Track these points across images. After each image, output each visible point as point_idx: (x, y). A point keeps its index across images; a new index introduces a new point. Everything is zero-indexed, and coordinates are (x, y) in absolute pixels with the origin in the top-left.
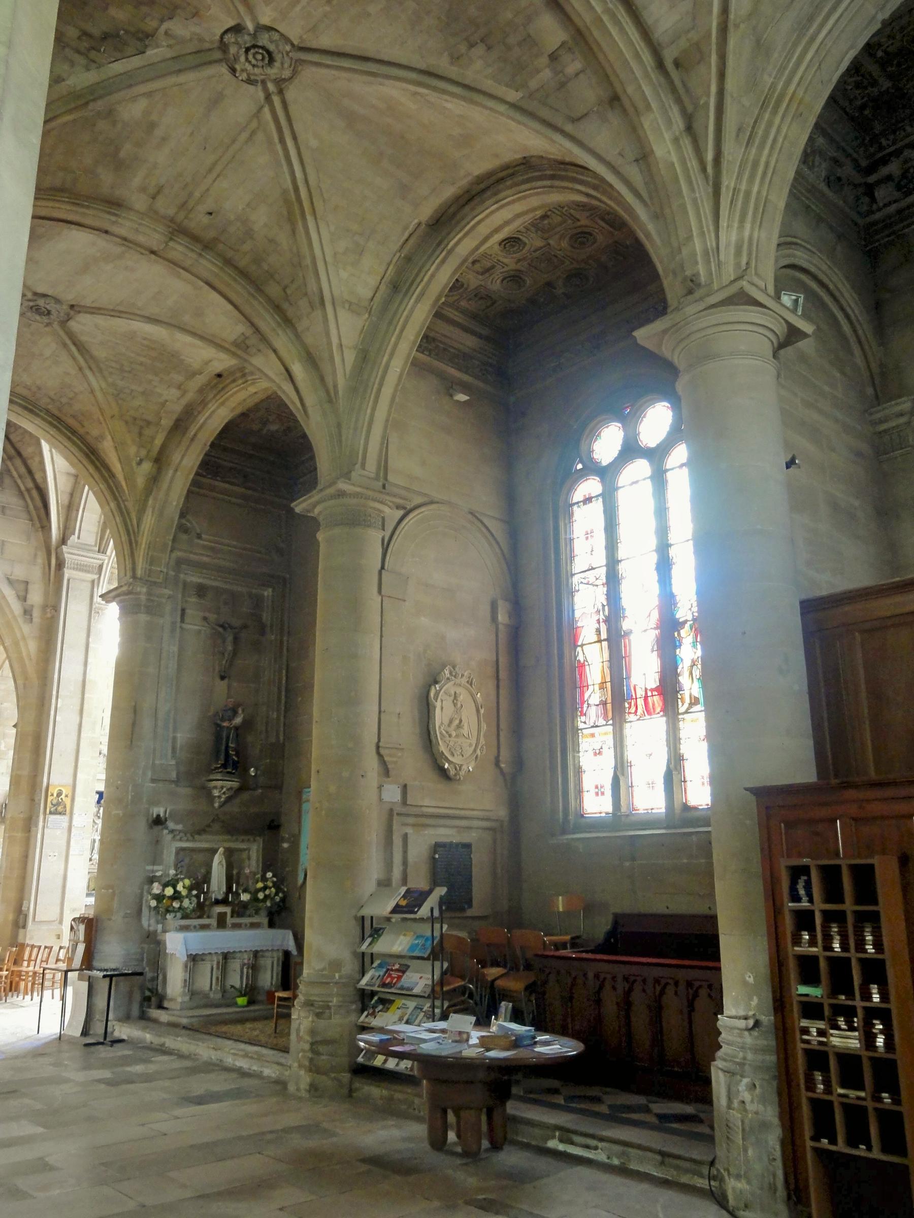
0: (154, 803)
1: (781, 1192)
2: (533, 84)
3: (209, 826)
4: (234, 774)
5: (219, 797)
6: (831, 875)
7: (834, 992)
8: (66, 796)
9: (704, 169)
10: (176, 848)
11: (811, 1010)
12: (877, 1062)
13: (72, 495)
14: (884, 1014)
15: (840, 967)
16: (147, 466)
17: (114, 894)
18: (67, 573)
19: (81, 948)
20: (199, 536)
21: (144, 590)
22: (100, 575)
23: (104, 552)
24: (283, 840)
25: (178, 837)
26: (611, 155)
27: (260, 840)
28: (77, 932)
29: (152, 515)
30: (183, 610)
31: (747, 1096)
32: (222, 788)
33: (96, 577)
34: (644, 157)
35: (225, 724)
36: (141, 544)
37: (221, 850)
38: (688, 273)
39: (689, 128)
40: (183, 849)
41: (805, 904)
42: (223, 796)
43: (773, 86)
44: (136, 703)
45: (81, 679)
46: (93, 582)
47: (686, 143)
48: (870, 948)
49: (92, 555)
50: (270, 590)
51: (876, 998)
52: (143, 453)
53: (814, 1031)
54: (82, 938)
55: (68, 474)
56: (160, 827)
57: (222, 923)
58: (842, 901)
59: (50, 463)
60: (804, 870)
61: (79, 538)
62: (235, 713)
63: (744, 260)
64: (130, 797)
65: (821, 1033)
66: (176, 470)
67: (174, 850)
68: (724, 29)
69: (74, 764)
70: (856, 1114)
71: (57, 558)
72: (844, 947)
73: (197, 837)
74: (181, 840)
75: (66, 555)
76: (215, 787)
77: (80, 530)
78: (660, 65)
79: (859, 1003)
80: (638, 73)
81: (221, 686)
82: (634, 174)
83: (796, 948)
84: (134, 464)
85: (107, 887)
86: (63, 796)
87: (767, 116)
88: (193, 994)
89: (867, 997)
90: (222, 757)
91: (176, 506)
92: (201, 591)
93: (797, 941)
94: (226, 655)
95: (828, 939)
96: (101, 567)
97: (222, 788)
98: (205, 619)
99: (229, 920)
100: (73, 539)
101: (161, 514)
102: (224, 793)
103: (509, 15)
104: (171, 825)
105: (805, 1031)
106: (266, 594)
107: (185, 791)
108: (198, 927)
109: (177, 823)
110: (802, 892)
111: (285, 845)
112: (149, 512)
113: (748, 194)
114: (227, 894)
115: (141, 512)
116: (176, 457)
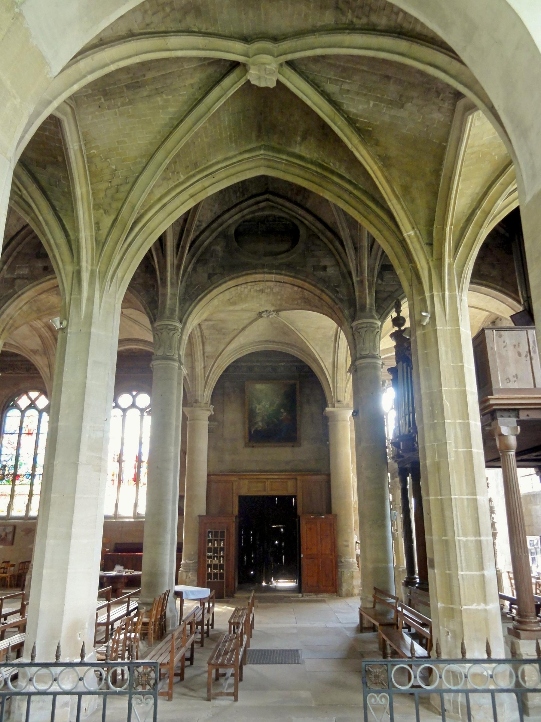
6: (216, 533)
7: (214, 553)
11: (210, 557)
12: (220, 565)
14: (223, 557)
15: (216, 549)
31: (190, 576)
38: (197, 398)
39: (204, 368)
41: (210, 538)
47: (203, 370)
48: (222, 546)
58: (218, 537)
60: (212, 532)
68: (219, 356)
70: (216, 574)
78: (204, 354)
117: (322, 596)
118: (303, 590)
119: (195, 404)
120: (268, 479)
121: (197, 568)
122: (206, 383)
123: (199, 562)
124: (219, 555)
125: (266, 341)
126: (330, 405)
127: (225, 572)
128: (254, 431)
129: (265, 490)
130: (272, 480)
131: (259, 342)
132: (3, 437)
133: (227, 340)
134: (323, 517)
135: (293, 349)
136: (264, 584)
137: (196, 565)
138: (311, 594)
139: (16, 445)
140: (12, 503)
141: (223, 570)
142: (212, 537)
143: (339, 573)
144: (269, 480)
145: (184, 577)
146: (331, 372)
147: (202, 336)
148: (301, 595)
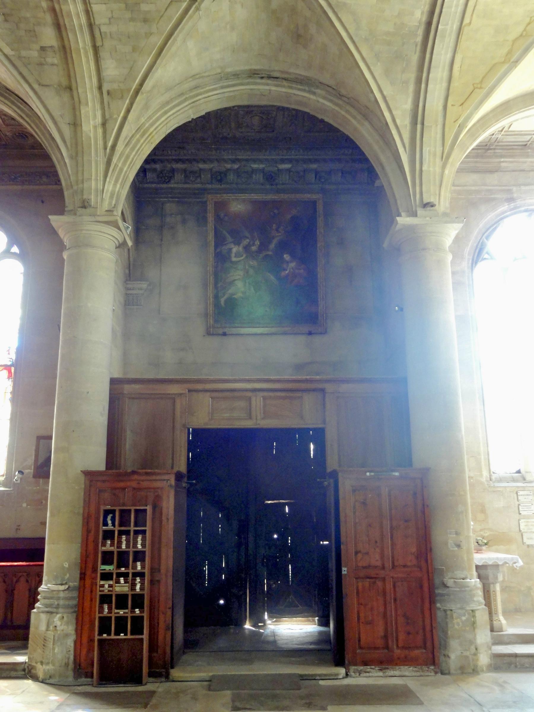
1: (71, 666)
2: (24, 53)
6: (125, 513)
7: (119, 567)
9: (105, 148)
14: (141, 575)
26: (56, 114)
34: (76, 125)
38: (85, 197)
41: (110, 527)
43: (144, 124)
47: (100, 131)
48: (139, 546)
51: (139, 568)
53: (106, 586)
58: (130, 526)
60: (113, 512)
63: (114, 202)
65: (110, 586)
68: (137, 92)
72: (128, 546)
78: (100, 88)
79: (131, 571)
80: (88, 85)
82: (67, 131)
83: (103, 548)
87: (138, 136)
89: (135, 567)
93: (104, 545)
95: (120, 543)
103: (28, 15)
105: (103, 586)
110: (110, 522)
113: (121, 170)
117: (397, 673)
118: (348, 657)
119: (81, 211)
120: (255, 390)
121: (75, 602)
122: (109, 163)
123: (81, 589)
124: (131, 571)
125: (253, 74)
126: (403, 214)
127: (146, 615)
128: (226, 301)
129: (250, 418)
130: (266, 394)
131: (236, 75)
133: (157, 40)
134: (397, 474)
135: (314, 93)
136: (248, 626)
137: (75, 594)
138: (368, 668)
141: (142, 611)
142: (114, 525)
143: (440, 614)
144: (262, 394)
145: (43, 627)
146: (406, 136)
147: (91, 26)
148: (342, 671)
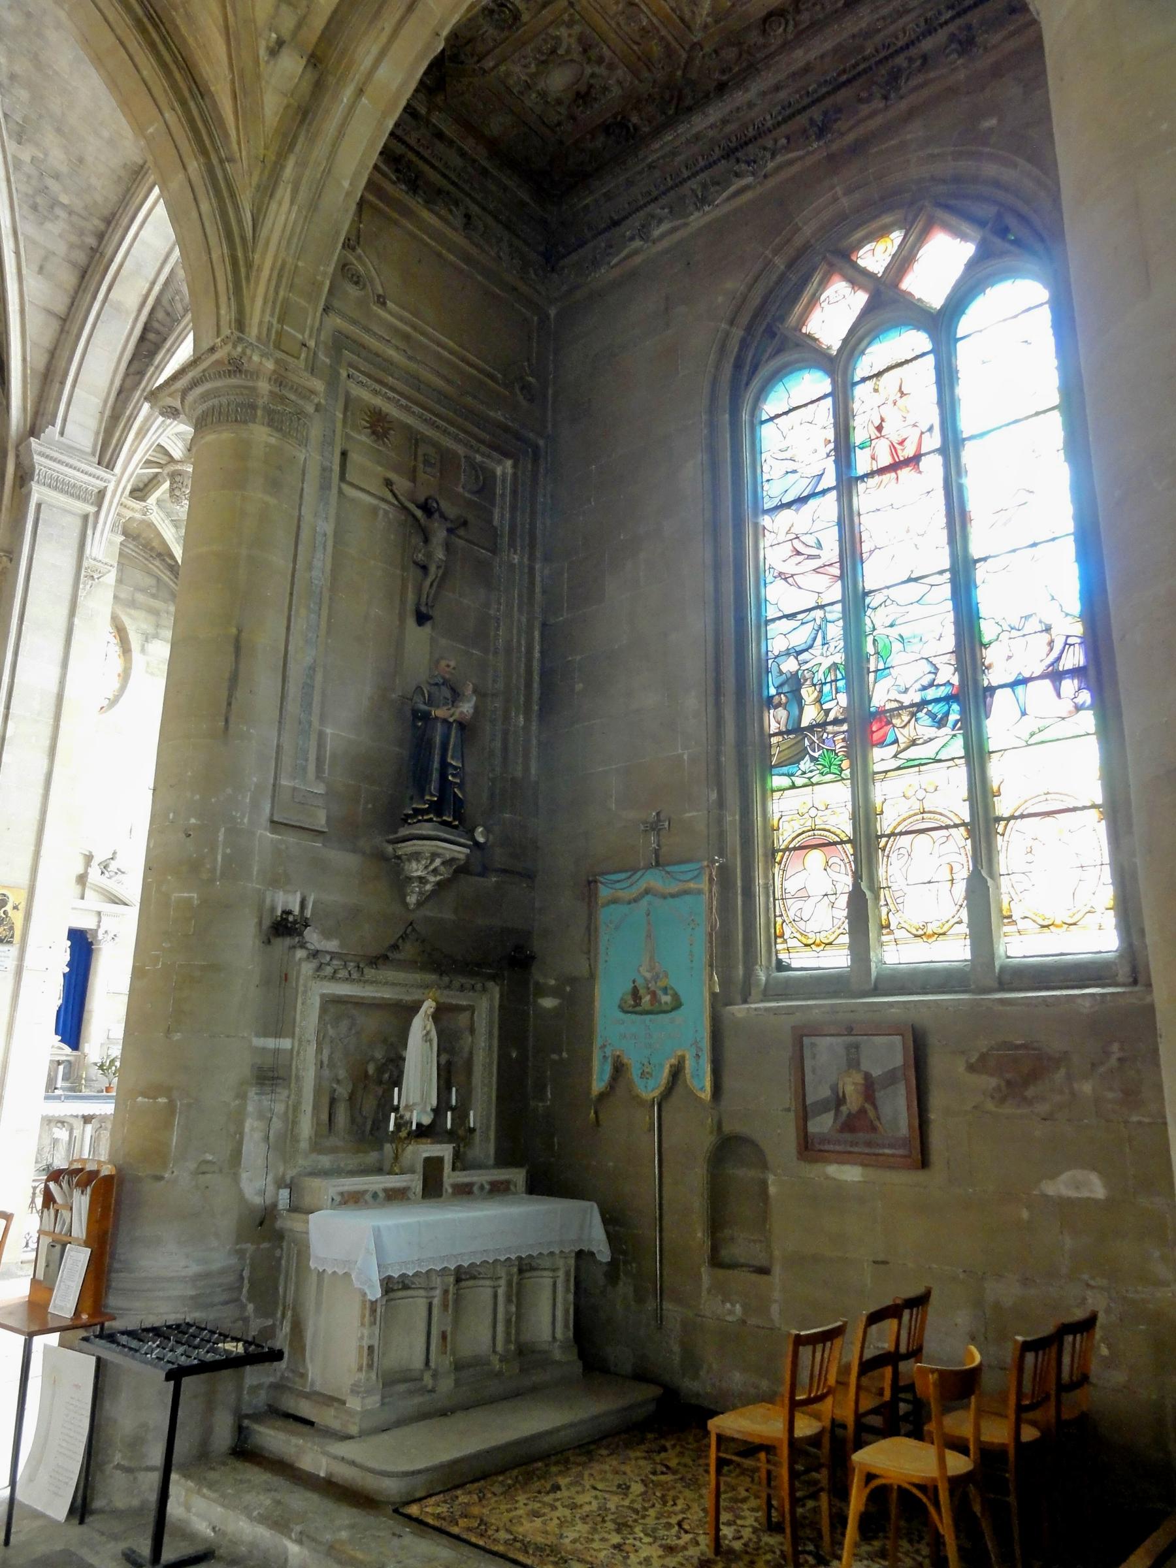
0: (276, 881)
3: (395, 947)
4: (456, 827)
5: (422, 880)
8: (15, 908)
10: (323, 996)
13: (53, 354)
16: (291, 65)
17: (171, 1105)
18: (38, 492)
19: (78, 1259)
20: (381, 301)
21: (270, 365)
22: (100, 506)
23: (110, 466)
24: (541, 991)
25: (329, 970)
27: (495, 991)
28: (65, 1213)
29: (292, 202)
30: (344, 454)
32: (434, 856)
33: (92, 509)
35: (439, 712)
36: (260, 269)
37: (428, 1006)
40: (338, 1001)
42: (432, 879)
44: (240, 631)
45: (54, 688)
46: (85, 518)
49: (84, 467)
50: (509, 463)
52: (288, 21)
54: (79, 1229)
55: (50, 312)
56: (288, 941)
57: (432, 1187)
59: (15, 277)
61: (62, 433)
62: (456, 695)
64: (219, 858)
66: (360, 92)
67: (317, 1002)
69: (32, 848)
71: (18, 465)
73: (370, 973)
74: (333, 977)
75: (36, 457)
76: (416, 856)
77: (65, 420)
81: (418, 638)
84: (263, 53)
85: (152, 1091)
86: (9, 907)
88: (392, 1381)
90: (434, 786)
91: (348, 194)
92: (378, 425)
94: (433, 569)
96: (101, 494)
97: (434, 856)
98: (388, 483)
99: (450, 1177)
100: (52, 432)
101: (313, 206)
102: (435, 872)
104: (312, 937)
106: (499, 471)
107: (344, 860)
108: (381, 1195)
109: (327, 934)
111: (548, 1003)
112: (284, 192)
114: (438, 1112)
115: (267, 190)
116: (366, 52)
132: (759, 532)
139: (831, 552)
140: (876, 890)
